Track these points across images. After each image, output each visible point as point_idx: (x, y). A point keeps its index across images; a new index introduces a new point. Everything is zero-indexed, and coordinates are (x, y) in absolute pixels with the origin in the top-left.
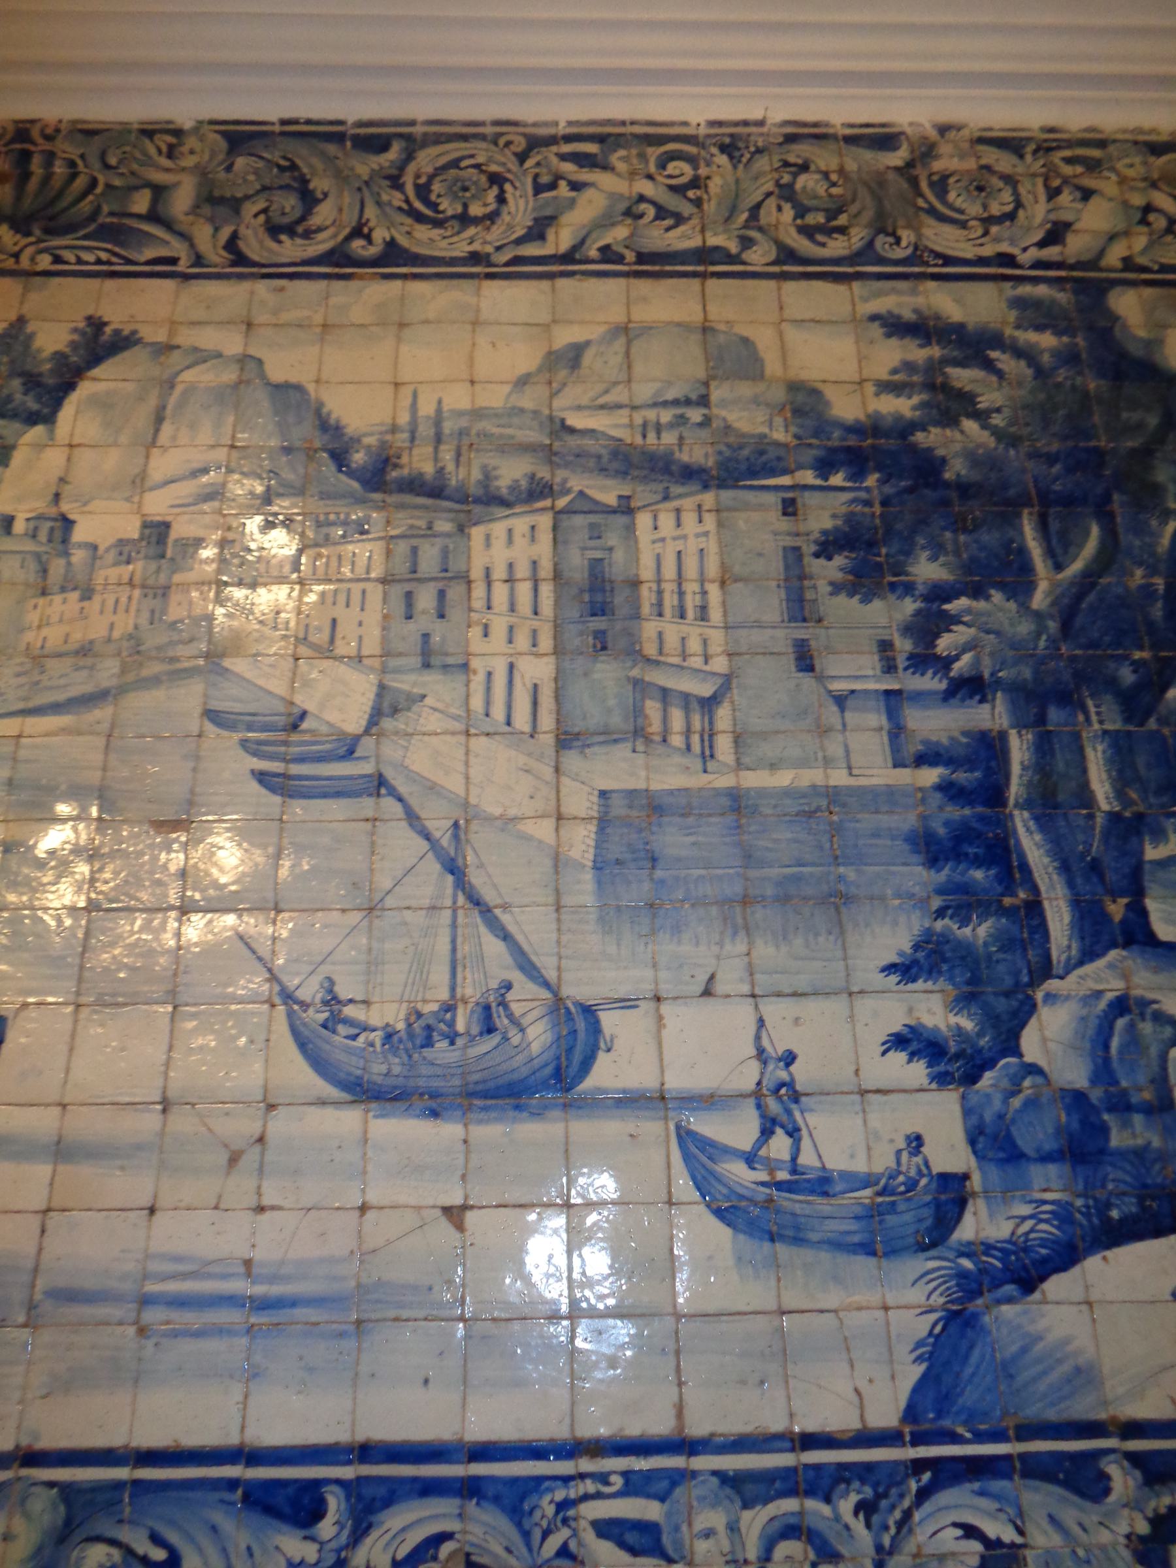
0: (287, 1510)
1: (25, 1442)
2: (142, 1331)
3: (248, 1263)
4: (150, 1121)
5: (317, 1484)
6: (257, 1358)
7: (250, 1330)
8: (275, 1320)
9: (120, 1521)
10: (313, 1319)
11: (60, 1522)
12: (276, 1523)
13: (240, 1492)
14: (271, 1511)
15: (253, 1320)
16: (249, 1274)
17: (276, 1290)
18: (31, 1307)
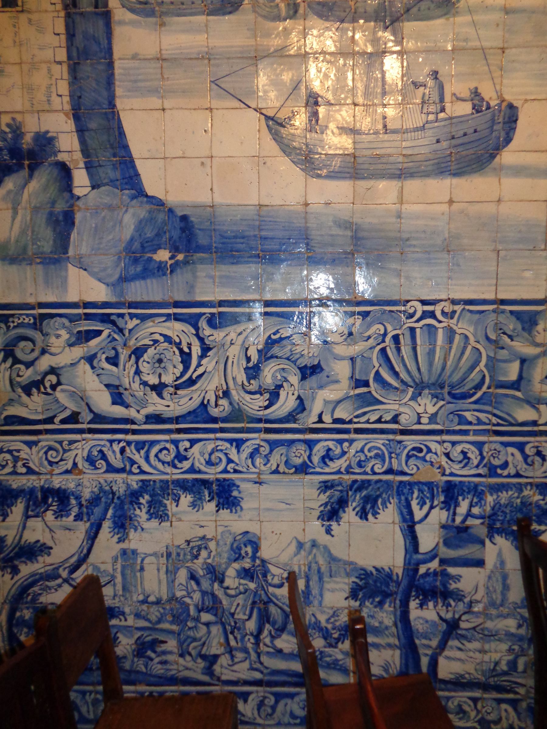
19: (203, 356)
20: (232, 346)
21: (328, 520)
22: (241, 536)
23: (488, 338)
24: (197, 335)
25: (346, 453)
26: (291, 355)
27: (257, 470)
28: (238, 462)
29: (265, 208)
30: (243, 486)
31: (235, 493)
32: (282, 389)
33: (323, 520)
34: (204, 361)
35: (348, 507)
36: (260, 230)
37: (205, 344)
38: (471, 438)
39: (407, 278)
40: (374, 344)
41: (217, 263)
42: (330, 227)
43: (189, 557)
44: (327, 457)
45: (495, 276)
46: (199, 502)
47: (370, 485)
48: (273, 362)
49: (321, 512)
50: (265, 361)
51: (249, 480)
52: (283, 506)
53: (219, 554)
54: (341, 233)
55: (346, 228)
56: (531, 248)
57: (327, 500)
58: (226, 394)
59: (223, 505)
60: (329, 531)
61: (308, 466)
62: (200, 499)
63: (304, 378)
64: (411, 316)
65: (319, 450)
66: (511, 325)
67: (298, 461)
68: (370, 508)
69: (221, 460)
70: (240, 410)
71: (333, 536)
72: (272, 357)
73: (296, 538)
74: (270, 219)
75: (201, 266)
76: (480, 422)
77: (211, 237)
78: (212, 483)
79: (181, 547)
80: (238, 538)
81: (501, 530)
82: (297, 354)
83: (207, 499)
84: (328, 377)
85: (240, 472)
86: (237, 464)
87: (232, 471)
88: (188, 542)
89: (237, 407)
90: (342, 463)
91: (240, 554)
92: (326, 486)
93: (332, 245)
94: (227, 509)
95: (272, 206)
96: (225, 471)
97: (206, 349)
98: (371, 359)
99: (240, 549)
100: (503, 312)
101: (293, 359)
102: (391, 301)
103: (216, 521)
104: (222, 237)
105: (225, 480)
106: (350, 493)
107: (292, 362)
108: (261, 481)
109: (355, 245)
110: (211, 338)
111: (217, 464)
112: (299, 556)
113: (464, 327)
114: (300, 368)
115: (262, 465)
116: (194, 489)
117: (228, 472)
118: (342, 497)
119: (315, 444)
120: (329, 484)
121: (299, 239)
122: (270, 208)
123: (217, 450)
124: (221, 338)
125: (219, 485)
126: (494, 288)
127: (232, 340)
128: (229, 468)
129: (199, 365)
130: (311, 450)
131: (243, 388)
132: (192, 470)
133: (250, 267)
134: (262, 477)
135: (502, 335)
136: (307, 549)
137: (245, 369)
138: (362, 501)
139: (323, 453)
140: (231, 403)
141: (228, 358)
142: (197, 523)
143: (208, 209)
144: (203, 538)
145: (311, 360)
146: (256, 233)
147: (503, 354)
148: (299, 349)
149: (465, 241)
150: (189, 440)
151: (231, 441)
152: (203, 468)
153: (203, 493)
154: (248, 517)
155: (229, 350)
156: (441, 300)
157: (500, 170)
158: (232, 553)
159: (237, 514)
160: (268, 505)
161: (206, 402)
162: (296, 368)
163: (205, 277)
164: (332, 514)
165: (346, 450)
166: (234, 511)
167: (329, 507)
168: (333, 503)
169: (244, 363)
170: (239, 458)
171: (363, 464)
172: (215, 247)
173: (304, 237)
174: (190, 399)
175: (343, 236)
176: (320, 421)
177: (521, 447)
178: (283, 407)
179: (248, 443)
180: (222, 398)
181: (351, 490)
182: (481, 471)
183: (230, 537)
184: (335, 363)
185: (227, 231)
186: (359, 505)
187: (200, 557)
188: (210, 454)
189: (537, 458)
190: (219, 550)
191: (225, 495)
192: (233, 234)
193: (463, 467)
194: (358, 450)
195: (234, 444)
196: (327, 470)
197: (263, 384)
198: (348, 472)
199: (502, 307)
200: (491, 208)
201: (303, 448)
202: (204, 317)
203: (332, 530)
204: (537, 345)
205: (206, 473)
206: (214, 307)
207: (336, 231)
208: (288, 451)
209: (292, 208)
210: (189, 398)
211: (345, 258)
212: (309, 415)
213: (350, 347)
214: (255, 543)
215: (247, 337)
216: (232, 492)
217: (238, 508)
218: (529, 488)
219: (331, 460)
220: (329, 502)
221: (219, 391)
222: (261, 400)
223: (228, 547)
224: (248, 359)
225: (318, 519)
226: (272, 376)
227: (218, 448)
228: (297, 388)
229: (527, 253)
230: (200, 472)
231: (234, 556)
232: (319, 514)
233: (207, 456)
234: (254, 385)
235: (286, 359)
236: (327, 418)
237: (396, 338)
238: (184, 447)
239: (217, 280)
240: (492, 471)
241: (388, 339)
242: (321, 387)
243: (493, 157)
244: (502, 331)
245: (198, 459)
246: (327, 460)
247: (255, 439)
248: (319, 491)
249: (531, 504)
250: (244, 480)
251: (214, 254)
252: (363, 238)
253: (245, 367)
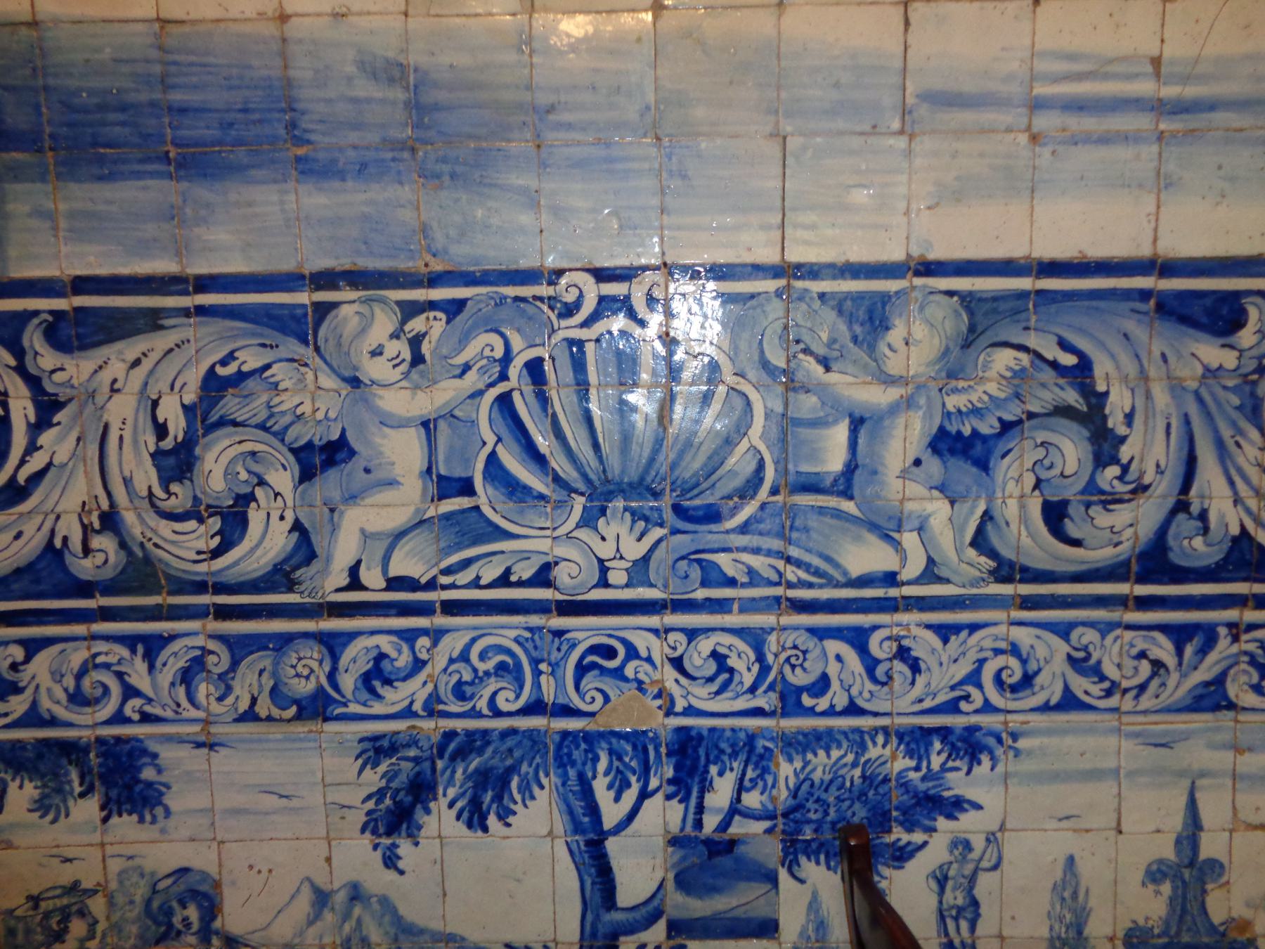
0: (1204, 320)
1: (916, 252)
2: (1034, 139)
3: (1156, 62)
5: (1237, 295)
6: (1170, 167)
7: (1160, 137)
8: (1192, 125)
9: (1027, 328)
10: (1237, 125)
11: (964, 329)
12: (1191, 331)
13: (1152, 302)
14: (1187, 320)
15: (1162, 126)
16: (1158, 75)
17: (1192, 91)
18: (905, 112)
19: (42, 422)
20: (116, 397)
21: (389, 834)
22: (169, 881)
23: (765, 365)
24: (21, 370)
25: (424, 663)
26: (271, 416)
27: (201, 714)
28: (151, 694)
29: (171, 29)
30: (167, 754)
31: (148, 774)
32: (253, 505)
33: (374, 832)
34: (46, 438)
35: (435, 799)
36: (167, 87)
37: (45, 393)
38: (734, 619)
39: (556, 211)
40: (481, 386)
41: (59, 176)
42: (350, 79)
43: (40, 938)
44: (377, 675)
45: (779, 203)
46: (57, 800)
47: (488, 743)
48: (228, 436)
49: (369, 813)
50: (204, 435)
51: (180, 740)
52: (273, 801)
53: (116, 928)
54: (378, 95)
55: (391, 80)
56: (867, 128)
57: (383, 783)
58: (110, 521)
59: (119, 803)
60: (391, 861)
61: (329, 700)
62: (59, 791)
63: (306, 475)
64: (569, 310)
65: (356, 657)
67: (304, 688)
68: (492, 801)
69: (106, 690)
70: (147, 560)
71: (402, 873)
72: (222, 423)
73: (308, 879)
74: (193, 58)
75: (19, 187)
76: (754, 578)
77: (37, 107)
78: (86, 750)
79: (19, 913)
80: (161, 886)
81: (814, 846)
82: (283, 413)
83: (78, 789)
84: (367, 471)
85: (157, 720)
86: (150, 701)
87: (136, 717)
88: (35, 900)
89: (140, 554)
90: (414, 690)
91: (170, 926)
92: (377, 749)
93: (357, 126)
94: (130, 814)
95: (194, 22)
96: (119, 718)
97: (48, 407)
98: (474, 423)
99: (169, 913)
100: (803, 296)
101: (276, 428)
102: (517, 271)
103: (102, 845)
104: (68, 106)
105: (118, 740)
106: (440, 764)
107: (275, 434)
108: (212, 740)
109: (417, 126)
110: (58, 377)
111: (97, 701)
112: (319, 923)
114: (292, 450)
115: (212, 699)
116: (42, 768)
117: (128, 721)
118: (418, 774)
119: (345, 645)
120: (385, 743)
121: (270, 110)
122: (186, 29)
123: (96, 666)
124: (85, 376)
125: (104, 755)
126: (779, 233)
127: (115, 381)
128: (128, 711)
129: (32, 448)
130: (335, 658)
131: (153, 505)
132: (33, 718)
133: (145, 188)
134: (213, 729)
135: (801, 356)
136: (337, 907)
137: (152, 455)
138: (470, 784)
139: (365, 666)
140: (123, 545)
141: (106, 427)
142: (55, 851)
143: (24, 31)
144: (74, 888)
145: (320, 429)
146: (157, 96)
147: (807, 405)
148: (287, 402)
149: (700, 113)
150: (21, 642)
151: (130, 641)
152: (62, 713)
153: (67, 774)
154: (185, 833)
155: (108, 405)
156: (645, 268)
158: (150, 923)
159: (158, 826)
160: (239, 800)
161: (58, 543)
162: (285, 450)
163: (30, 215)
164: (396, 817)
165: (424, 656)
166: (148, 817)
167: (388, 802)
168: (398, 791)
169: (151, 439)
170: (154, 685)
171: (468, 690)
172: (51, 136)
173: (283, 105)
174: (18, 536)
175: (383, 101)
176: (355, 583)
177: (858, 639)
178: (259, 552)
179: (176, 646)
180: (98, 532)
181: (441, 756)
182: (761, 701)
183: (142, 883)
184: (385, 436)
185: (80, 90)
186: (463, 794)
187: (68, 937)
188: (79, 676)
189: (899, 666)
190: (116, 917)
191: (125, 781)
192: (95, 100)
193: (717, 693)
194: (455, 655)
195: (140, 649)
196: (378, 708)
197: (204, 493)
198: (431, 713)
199: (799, 284)
201: (316, 655)
202: (36, 321)
203: (399, 858)
204: (889, 380)
205: (70, 725)
206: (61, 294)
207: (364, 88)
208: (276, 664)
209: (247, 28)
210: (14, 533)
211: (394, 160)
212: (325, 571)
213: (420, 394)
214: (205, 896)
215: (151, 372)
216: (139, 770)
217: (159, 811)
218: (880, 739)
219: (388, 682)
220: (388, 787)
221: (90, 512)
222: (200, 536)
223: (138, 910)
224: (161, 430)
225: (363, 831)
226: (226, 473)
227: (99, 660)
228: (290, 503)
229: (856, 142)
230: (53, 722)
231: (154, 931)
232: (365, 819)
233: (70, 682)
234: (180, 496)
235: (257, 426)
236: (372, 577)
237: (535, 369)
238: (10, 660)
239: (63, 224)
240: (790, 701)
241: (515, 370)
242: (352, 498)
244: (802, 346)
245: (49, 690)
246: (377, 684)
247: (193, 635)
248: (360, 761)
249: (886, 780)
250: (169, 739)
251: (50, 154)
252: (436, 107)
253: (152, 449)
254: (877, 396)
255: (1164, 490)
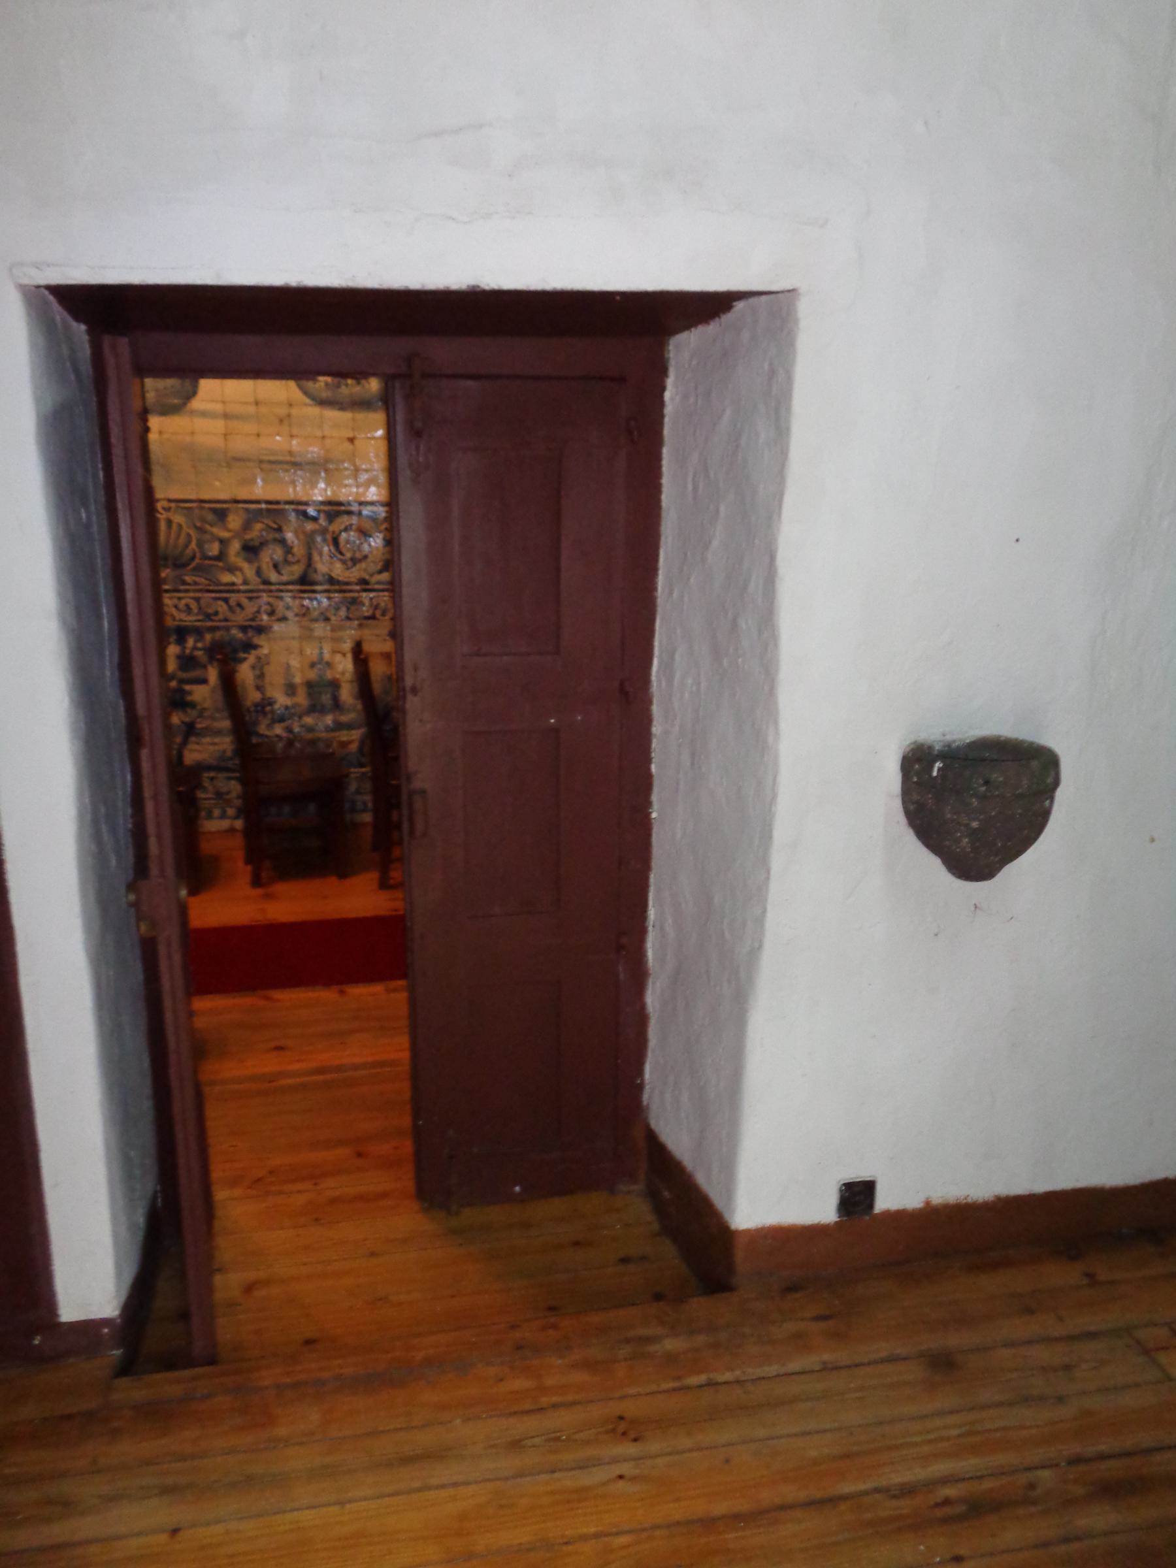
4: (252, 409)
38: (192, 595)
66: (210, 517)
76: (196, 583)
113: (178, 519)
147: (207, 537)
157: (193, 413)
177: (226, 600)
182: (200, 617)
200: (188, 439)
204: (229, 531)
240: (208, 617)
243: (185, 404)
254: (225, 535)
255: (304, 561)
